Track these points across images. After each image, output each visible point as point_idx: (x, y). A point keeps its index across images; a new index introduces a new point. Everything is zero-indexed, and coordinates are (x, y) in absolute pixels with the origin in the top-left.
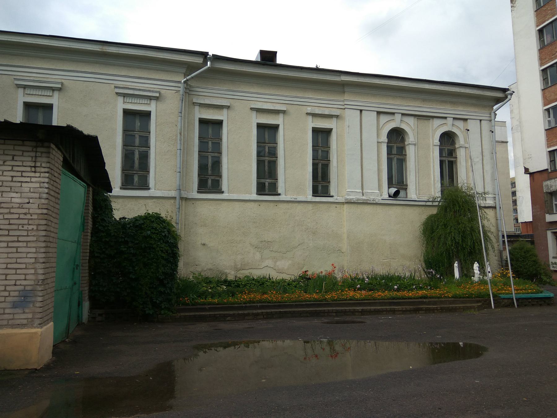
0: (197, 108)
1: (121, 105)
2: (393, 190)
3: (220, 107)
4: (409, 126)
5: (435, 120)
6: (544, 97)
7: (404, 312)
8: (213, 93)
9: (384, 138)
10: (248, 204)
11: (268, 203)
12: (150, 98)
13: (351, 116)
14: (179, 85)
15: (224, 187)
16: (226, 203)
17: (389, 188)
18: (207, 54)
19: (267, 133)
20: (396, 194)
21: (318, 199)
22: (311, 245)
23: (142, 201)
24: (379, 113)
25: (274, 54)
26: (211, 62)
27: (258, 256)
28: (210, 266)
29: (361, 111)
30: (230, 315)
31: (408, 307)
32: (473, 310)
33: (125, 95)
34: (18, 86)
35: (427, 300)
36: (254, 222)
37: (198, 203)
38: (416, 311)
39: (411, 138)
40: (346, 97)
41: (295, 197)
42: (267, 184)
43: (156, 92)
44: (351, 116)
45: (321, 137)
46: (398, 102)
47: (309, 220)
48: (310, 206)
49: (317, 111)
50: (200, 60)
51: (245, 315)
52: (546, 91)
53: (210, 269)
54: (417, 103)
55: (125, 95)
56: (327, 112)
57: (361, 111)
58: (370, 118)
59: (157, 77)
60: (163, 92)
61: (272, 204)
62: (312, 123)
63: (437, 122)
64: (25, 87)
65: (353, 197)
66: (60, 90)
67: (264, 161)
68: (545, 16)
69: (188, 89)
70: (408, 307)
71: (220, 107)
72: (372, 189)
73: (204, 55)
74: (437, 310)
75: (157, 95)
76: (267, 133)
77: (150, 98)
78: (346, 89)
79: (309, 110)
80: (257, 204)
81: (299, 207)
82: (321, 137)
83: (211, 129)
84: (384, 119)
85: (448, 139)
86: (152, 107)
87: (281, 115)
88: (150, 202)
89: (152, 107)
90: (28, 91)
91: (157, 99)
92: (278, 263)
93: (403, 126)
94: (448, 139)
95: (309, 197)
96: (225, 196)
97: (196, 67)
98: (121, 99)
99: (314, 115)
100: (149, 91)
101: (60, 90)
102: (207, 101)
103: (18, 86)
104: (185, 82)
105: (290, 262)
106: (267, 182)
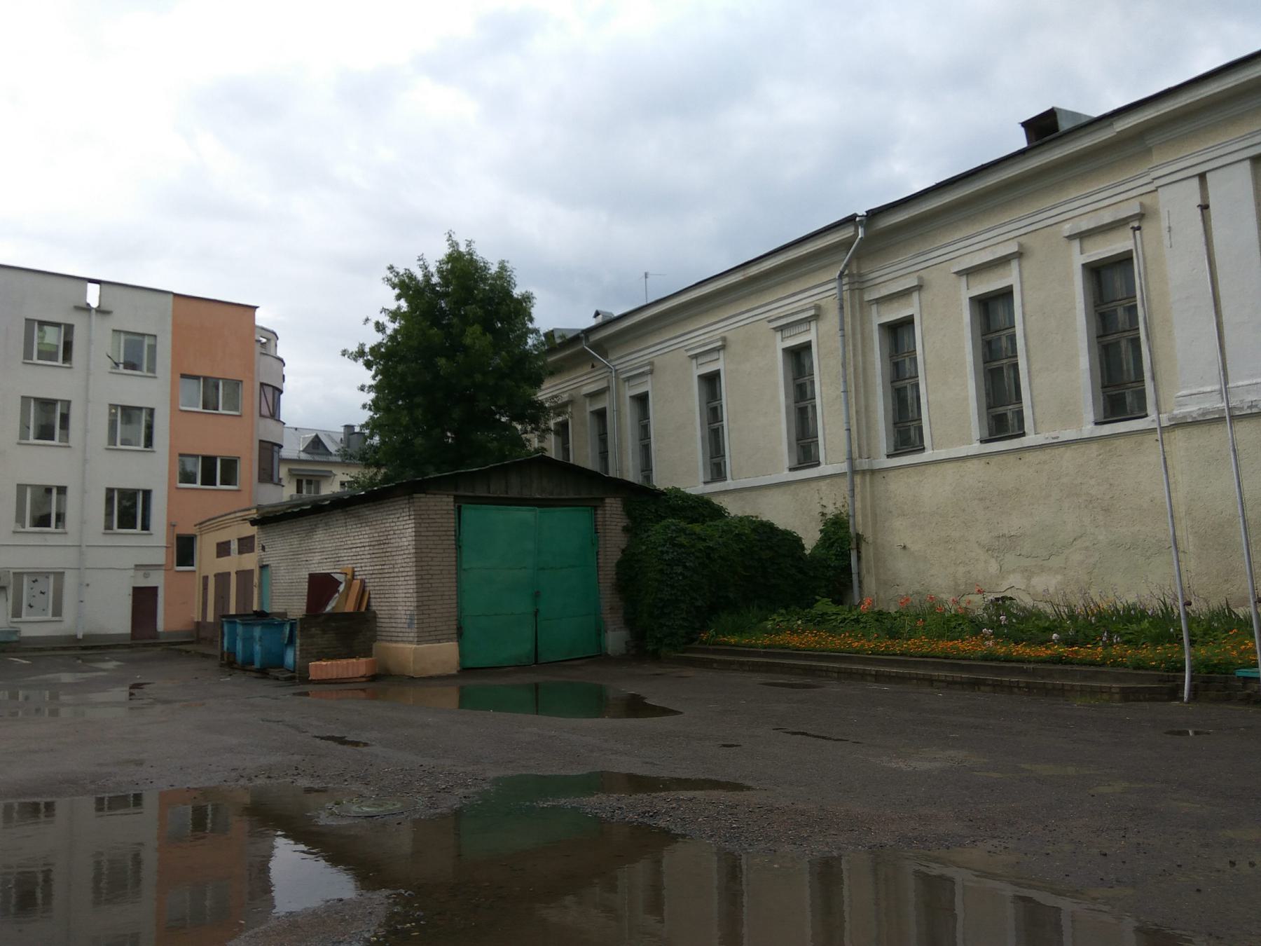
0: (874, 308)
3: (905, 293)
7: (951, 684)
8: (891, 274)
10: (972, 466)
11: (1005, 457)
12: (807, 320)
15: (927, 442)
16: (932, 469)
18: (855, 216)
19: (992, 310)
21: (1107, 429)
22: (1101, 538)
23: (814, 485)
25: (1051, 115)
26: (866, 228)
27: (993, 567)
28: (917, 587)
30: (716, 661)
31: (958, 675)
32: (1105, 696)
33: (781, 329)
35: (1032, 666)
36: (981, 499)
37: (891, 474)
38: (975, 684)
41: (1054, 434)
42: (1010, 415)
43: (810, 309)
47: (1093, 482)
49: (1085, 225)
50: (847, 233)
51: (742, 664)
53: (918, 593)
55: (781, 329)
56: (1107, 217)
59: (717, 319)
60: (822, 303)
61: (1012, 459)
62: (1079, 257)
64: (696, 357)
65: (1192, 409)
66: (723, 347)
67: (1001, 369)
69: (855, 282)
70: (958, 675)
71: (905, 293)
72: (1252, 376)
73: (851, 220)
74: (1019, 688)
75: (812, 312)
76: (992, 310)
77: (807, 320)
79: (1067, 229)
80: (983, 461)
81: (1068, 454)
86: (809, 335)
87: (915, 295)
88: (823, 485)
89: (809, 335)
90: (701, 360)
92: (1035, 581)
95: (1089, 429)
96: (1030, 439)
99: (1083, 236)
100: (803, 311)
101: (723, 347)
102: (884, 292)
105: (1059, 577)
106: (1009, 410)
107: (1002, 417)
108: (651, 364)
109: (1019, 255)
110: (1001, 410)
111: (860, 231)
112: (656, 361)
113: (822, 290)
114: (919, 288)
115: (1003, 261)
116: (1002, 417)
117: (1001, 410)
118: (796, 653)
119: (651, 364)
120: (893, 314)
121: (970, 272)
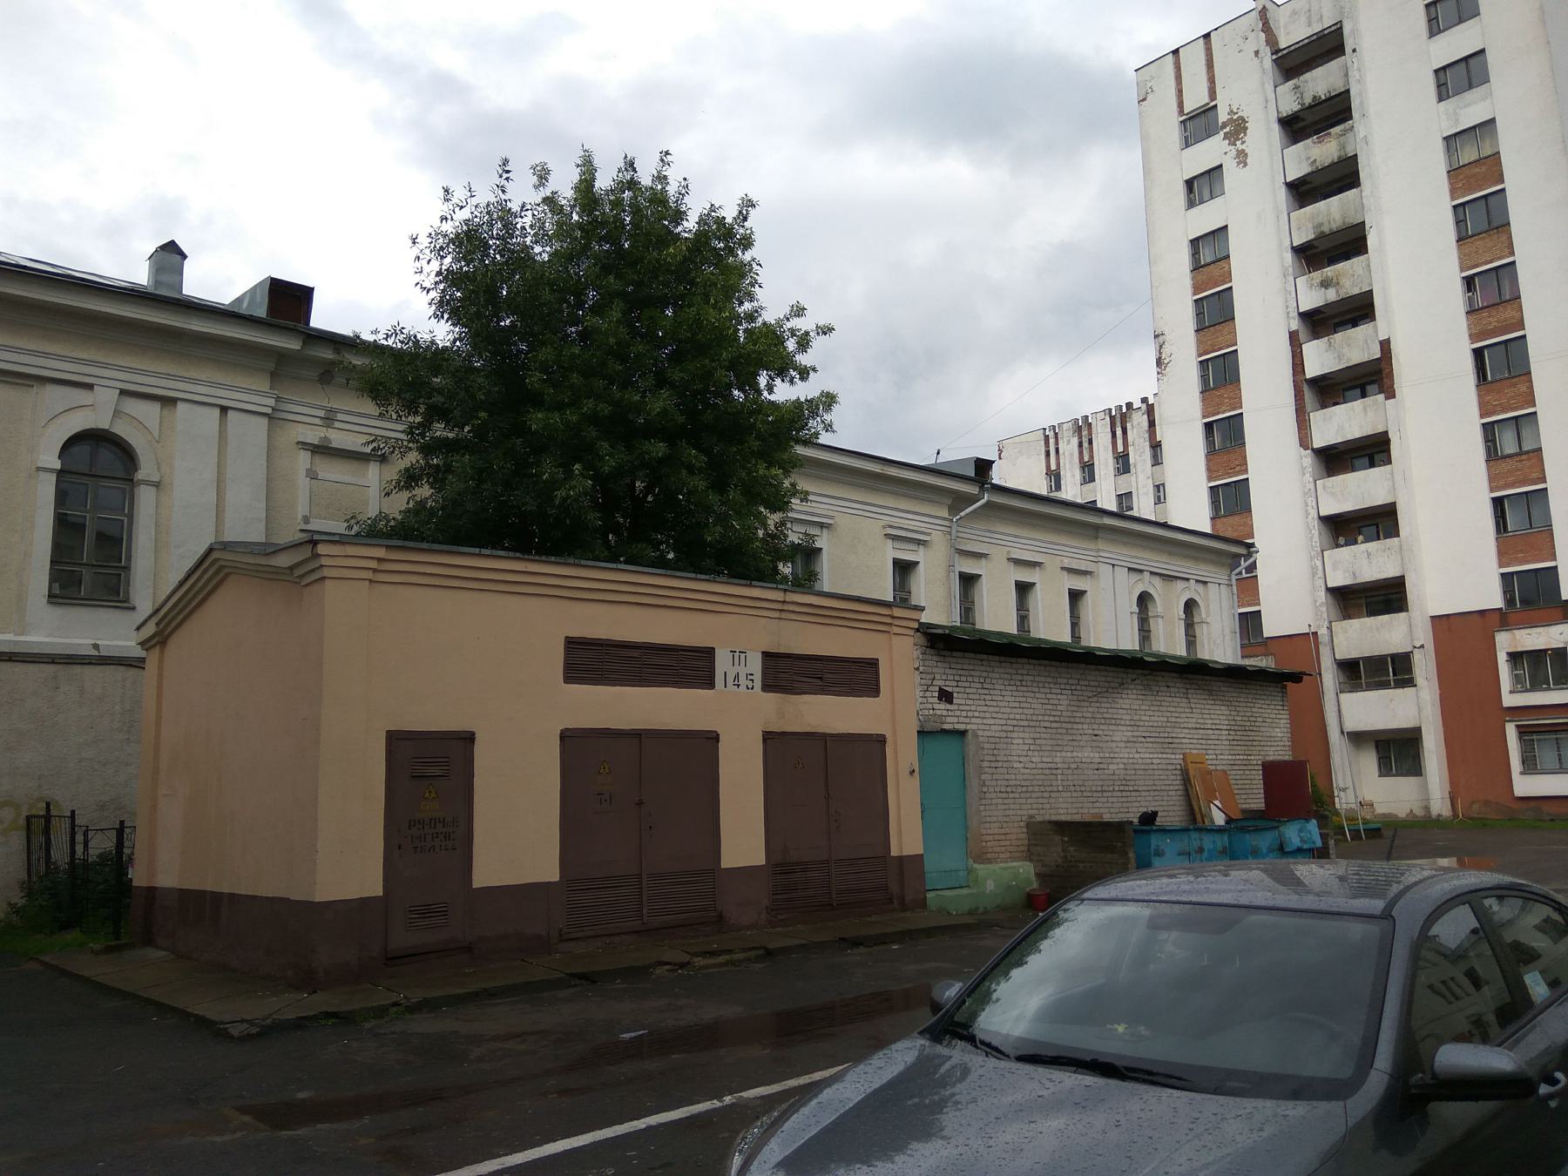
1: (891, 552)
4: (1156, 588)
12: (919, 542)
13: (1104, 570)
39: (1158, 607)
40: (1101, 545)
46: (1146, 555)
54: (1164, 558)
63: (1180, 585)
77: (919, 542)
79: (1067, 563)
84: (1135, 577)
85: (1190, 606)
93: (1151, 591)
98: (889, 542)
99: (1070, 571)
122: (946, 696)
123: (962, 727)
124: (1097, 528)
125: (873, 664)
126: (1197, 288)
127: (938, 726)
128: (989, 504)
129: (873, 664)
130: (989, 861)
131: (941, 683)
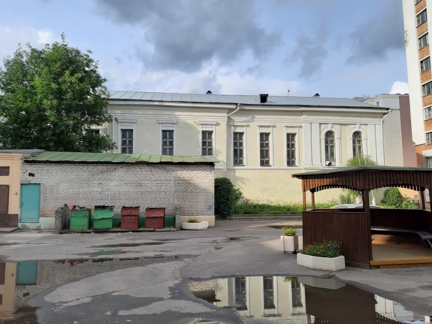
2: (328, 163)
4: (336, 130)
5: (350, 126)
6: (424, 102)
9: (323, 136)
12: (213, 125)
13: (306, 127)
14: (225, 118)
17: (326, 161)
19: (264, 137)
20: (330, 164)
24: (320, 124)
29: (311, 123)
34: (159, 123)
42: (265, 161)
44: (306, 127)
45: (291, 137)
48: (286, 171)
50: (234, 107)
52: (424, 98)
55: (202, 124)
56: (293, 125)
57: (311, 123)
58: (316, 127)
68: (424, 54)
76: (264, 137)
77: (213, 125)
78: (303, 113)
82: (291, 137)
83: (238, 136)
84: (322, 126)
85: (357, 134)
90: (163, 125)
91: (216, 125)
94: (357, 134)
97: (233, 110)
103: (159, 123)
104: (228, 117)
107: (264, 161)
108: (137, 120)
109: (274, 126)
110: (263, 159)
111: (238, 108)
112: (138, 119)
113: (221, 118)
114: (246, 126)
115: (269, 127)
116: (264, 161)
117: (263, 159)
118: (273, 216)
119: (137, 120)
120: (239, 130)
121: (261, 126)
122: (31, 175)
123: (39, 183)
124: (302, 111)
125: (8, 168)
126: (417, 11)
127: (28, 183)
128: (240, 110)
129: (8, 168)
130: (47, 217)
131: (31, 172)
